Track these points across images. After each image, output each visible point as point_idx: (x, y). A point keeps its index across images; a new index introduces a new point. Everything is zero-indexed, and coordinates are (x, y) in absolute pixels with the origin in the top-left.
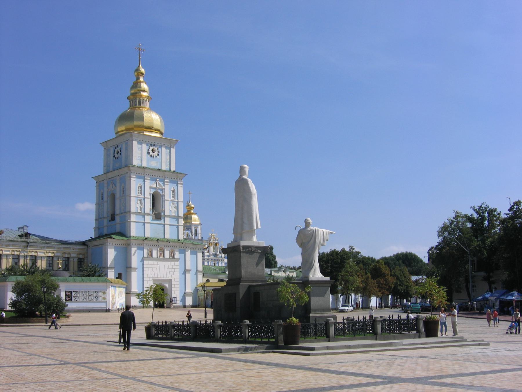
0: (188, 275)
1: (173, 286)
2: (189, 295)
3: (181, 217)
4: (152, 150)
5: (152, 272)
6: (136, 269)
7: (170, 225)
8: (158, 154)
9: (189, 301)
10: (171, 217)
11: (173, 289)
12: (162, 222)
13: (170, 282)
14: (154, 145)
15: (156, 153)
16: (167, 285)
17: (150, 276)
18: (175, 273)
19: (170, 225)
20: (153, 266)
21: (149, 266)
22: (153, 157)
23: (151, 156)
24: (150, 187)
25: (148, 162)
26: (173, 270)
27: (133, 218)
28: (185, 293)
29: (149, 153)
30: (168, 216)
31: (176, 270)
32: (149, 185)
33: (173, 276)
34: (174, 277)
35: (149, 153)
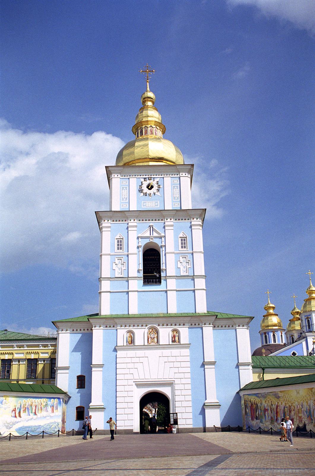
0: (210, 372)
1: (177, 393)
2: (217, 406)
3: (200, 277)
4: (148, 187)
5: (132, 371)
6: (101, 366)
7: (177, 291)
8: (158, 190)
9: (214, 418)
10: (178, 277)
11: (177, 398)
12: (162, 287)
13: (170, 384)
14: (150, 179)
15: (154, 190)
16: (166, 391)
17: (131, 377)
18: (181, 370)
19: (177, 291)
20: (134, 360)
21: (129, 360)
22: (150, 194)
23: (145, 194)
24: (138, 238)
25: (139, 202)
26: (178, 365)
27: (105, 286)
28: (204, 405)
29: (141, 191)
30: (171, 277)
31: (183, 364)
32: (136, 236)
33: (177, 376)
34: (182, 375)
35: (141, 191)
